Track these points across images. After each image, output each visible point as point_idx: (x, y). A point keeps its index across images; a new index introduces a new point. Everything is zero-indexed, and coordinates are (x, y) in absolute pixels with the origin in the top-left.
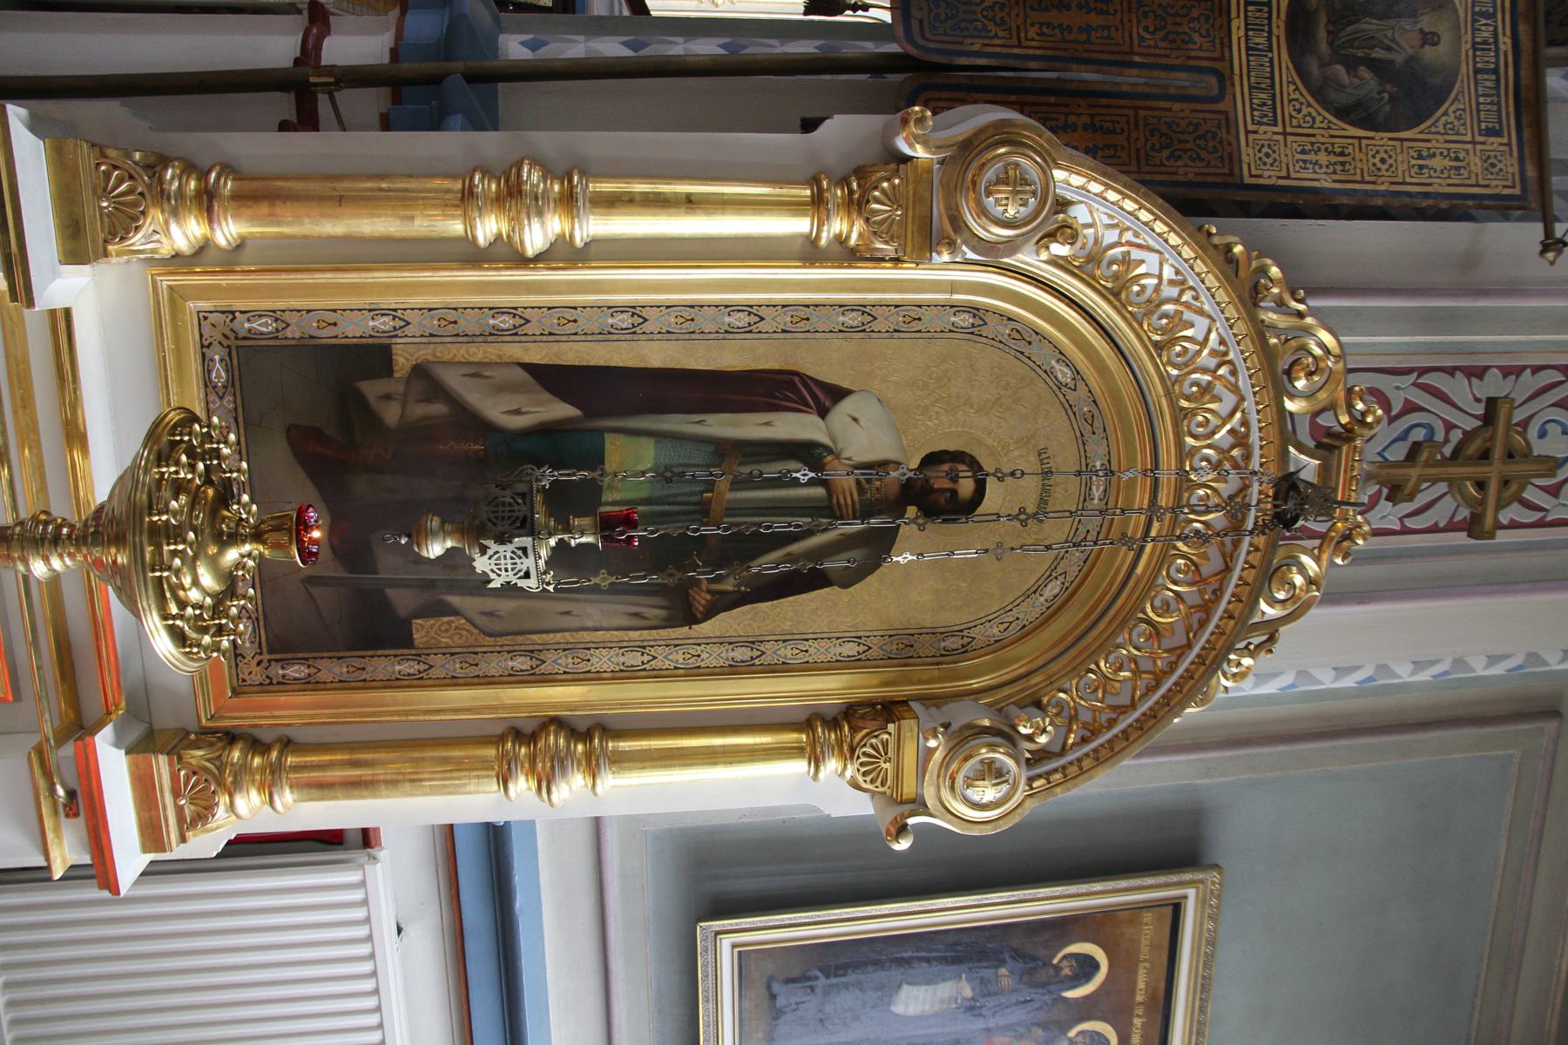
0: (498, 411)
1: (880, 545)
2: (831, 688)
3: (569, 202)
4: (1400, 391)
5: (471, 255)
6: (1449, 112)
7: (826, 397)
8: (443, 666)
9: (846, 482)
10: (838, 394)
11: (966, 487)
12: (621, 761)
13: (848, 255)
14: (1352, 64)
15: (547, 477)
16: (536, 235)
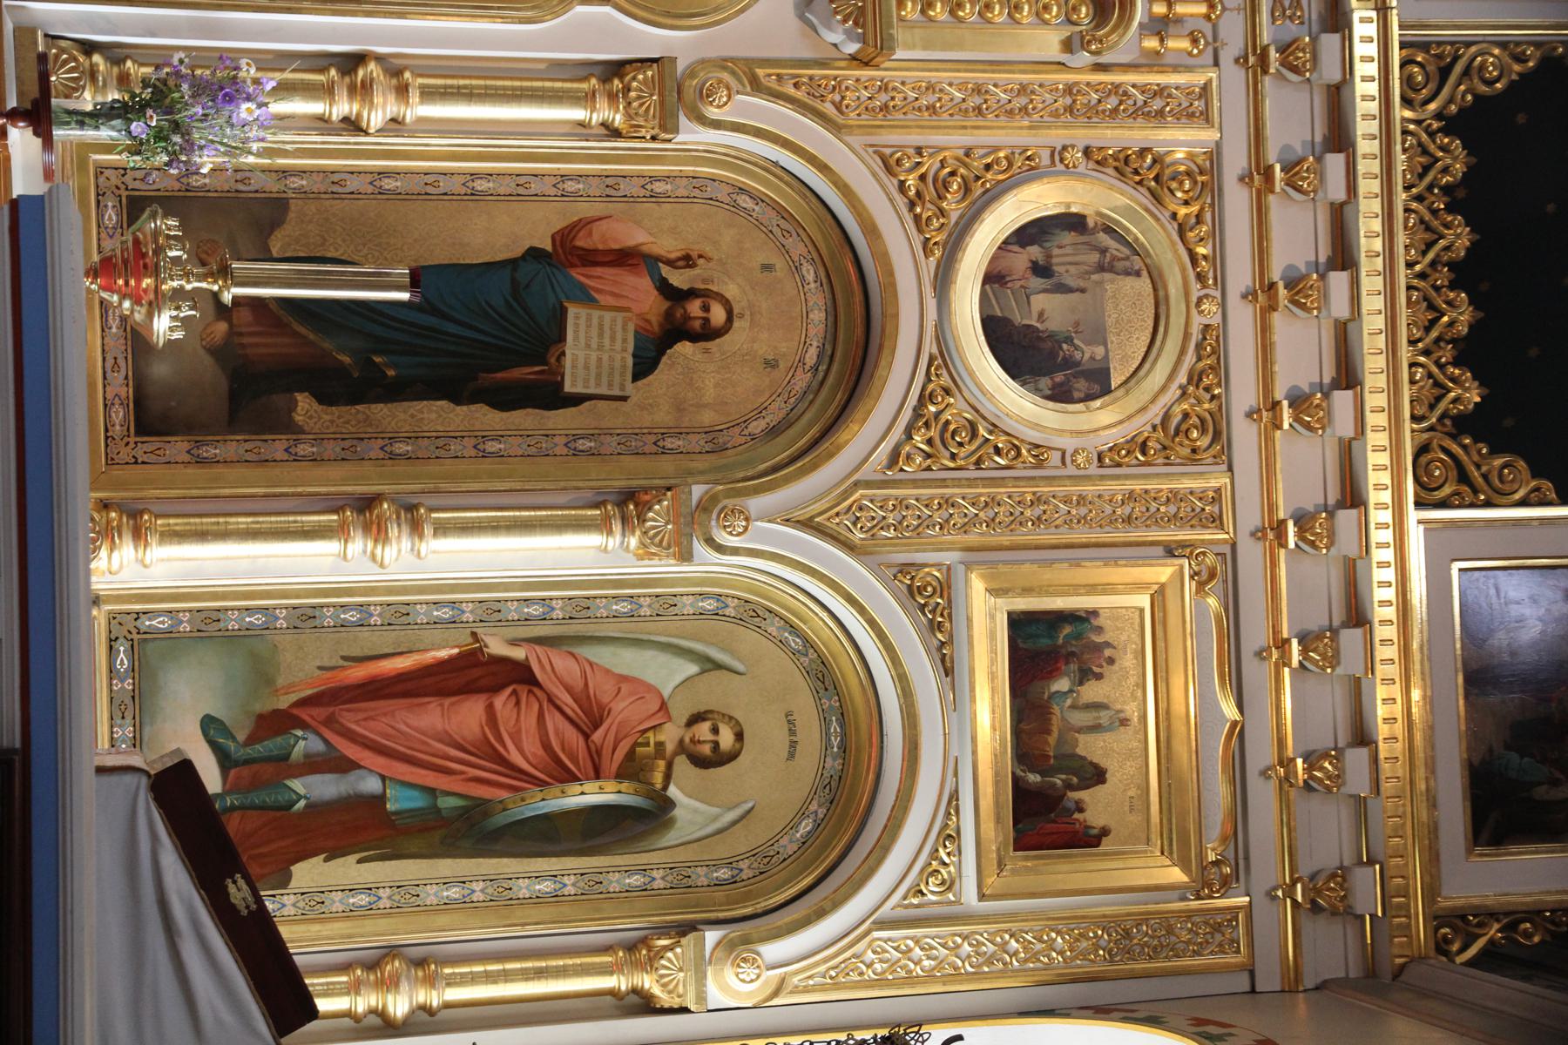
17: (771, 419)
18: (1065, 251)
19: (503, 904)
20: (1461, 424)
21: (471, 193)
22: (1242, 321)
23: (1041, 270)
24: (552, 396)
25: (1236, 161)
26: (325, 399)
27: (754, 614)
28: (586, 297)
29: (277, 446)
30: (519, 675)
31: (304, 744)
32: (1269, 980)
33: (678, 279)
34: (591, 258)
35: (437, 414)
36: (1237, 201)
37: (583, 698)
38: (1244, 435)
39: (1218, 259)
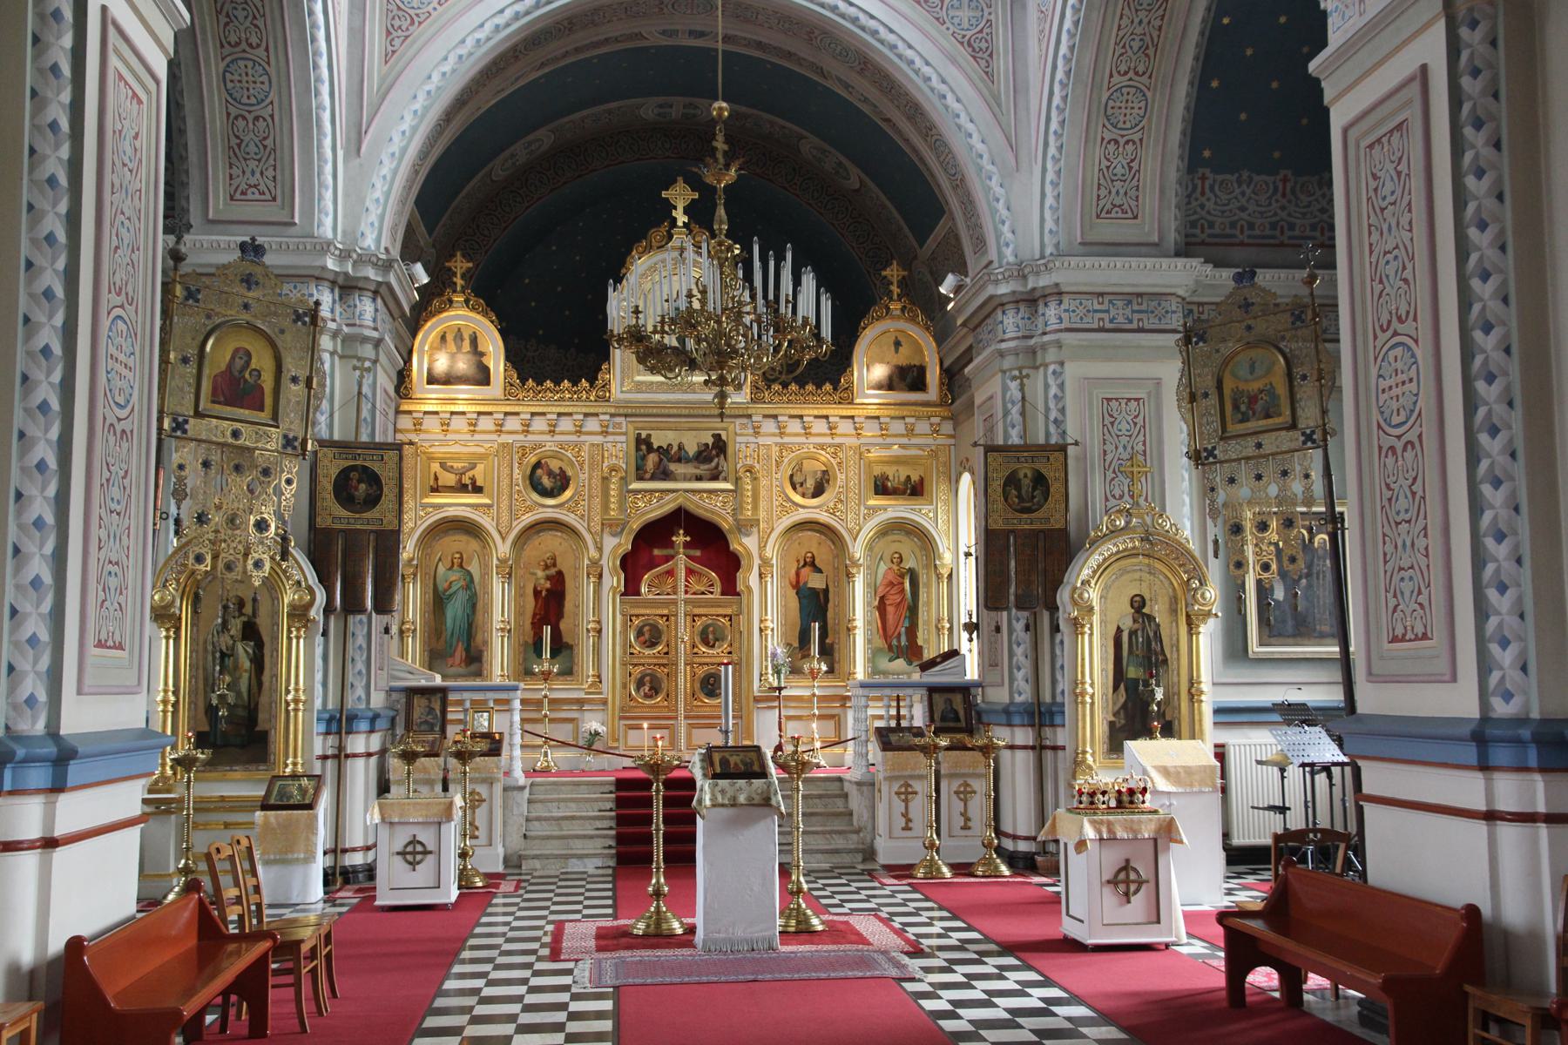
0: (1122, 700)
1: (1151, 618)
2: (1183, 629)
3: (1083, 683)
4: (1110, 475)
5: (1092, 704)
6: (1043, 471)
7: (1119, 630)
8: (1176, 715)
10: (1118, 628)
11: (1137, 599)
12: (1198, 676)
13: (1091, 629)
14: (1033, 497)
15: (1141, 688)
16: (1090, 690)
17: (830, 543)
18: (797, 479)
19: (928, 603)
20: (835, 389)
21: (785, 606)
22: (812, 440)
23: (802, 485)
24: (826, 591)
25: (778, 440)
26: (827, 637)
27: (870, 547)
28: (806, 583)
29: (836, 646)
30: (882, 599)
31: (895, 642)
32: (952, 441)
33: (802, 563)
34: (798, 582)
35: (830, 614)
36: (786, 440)
37: (887, 586)
38: (837, 440)
39: (799, 444)
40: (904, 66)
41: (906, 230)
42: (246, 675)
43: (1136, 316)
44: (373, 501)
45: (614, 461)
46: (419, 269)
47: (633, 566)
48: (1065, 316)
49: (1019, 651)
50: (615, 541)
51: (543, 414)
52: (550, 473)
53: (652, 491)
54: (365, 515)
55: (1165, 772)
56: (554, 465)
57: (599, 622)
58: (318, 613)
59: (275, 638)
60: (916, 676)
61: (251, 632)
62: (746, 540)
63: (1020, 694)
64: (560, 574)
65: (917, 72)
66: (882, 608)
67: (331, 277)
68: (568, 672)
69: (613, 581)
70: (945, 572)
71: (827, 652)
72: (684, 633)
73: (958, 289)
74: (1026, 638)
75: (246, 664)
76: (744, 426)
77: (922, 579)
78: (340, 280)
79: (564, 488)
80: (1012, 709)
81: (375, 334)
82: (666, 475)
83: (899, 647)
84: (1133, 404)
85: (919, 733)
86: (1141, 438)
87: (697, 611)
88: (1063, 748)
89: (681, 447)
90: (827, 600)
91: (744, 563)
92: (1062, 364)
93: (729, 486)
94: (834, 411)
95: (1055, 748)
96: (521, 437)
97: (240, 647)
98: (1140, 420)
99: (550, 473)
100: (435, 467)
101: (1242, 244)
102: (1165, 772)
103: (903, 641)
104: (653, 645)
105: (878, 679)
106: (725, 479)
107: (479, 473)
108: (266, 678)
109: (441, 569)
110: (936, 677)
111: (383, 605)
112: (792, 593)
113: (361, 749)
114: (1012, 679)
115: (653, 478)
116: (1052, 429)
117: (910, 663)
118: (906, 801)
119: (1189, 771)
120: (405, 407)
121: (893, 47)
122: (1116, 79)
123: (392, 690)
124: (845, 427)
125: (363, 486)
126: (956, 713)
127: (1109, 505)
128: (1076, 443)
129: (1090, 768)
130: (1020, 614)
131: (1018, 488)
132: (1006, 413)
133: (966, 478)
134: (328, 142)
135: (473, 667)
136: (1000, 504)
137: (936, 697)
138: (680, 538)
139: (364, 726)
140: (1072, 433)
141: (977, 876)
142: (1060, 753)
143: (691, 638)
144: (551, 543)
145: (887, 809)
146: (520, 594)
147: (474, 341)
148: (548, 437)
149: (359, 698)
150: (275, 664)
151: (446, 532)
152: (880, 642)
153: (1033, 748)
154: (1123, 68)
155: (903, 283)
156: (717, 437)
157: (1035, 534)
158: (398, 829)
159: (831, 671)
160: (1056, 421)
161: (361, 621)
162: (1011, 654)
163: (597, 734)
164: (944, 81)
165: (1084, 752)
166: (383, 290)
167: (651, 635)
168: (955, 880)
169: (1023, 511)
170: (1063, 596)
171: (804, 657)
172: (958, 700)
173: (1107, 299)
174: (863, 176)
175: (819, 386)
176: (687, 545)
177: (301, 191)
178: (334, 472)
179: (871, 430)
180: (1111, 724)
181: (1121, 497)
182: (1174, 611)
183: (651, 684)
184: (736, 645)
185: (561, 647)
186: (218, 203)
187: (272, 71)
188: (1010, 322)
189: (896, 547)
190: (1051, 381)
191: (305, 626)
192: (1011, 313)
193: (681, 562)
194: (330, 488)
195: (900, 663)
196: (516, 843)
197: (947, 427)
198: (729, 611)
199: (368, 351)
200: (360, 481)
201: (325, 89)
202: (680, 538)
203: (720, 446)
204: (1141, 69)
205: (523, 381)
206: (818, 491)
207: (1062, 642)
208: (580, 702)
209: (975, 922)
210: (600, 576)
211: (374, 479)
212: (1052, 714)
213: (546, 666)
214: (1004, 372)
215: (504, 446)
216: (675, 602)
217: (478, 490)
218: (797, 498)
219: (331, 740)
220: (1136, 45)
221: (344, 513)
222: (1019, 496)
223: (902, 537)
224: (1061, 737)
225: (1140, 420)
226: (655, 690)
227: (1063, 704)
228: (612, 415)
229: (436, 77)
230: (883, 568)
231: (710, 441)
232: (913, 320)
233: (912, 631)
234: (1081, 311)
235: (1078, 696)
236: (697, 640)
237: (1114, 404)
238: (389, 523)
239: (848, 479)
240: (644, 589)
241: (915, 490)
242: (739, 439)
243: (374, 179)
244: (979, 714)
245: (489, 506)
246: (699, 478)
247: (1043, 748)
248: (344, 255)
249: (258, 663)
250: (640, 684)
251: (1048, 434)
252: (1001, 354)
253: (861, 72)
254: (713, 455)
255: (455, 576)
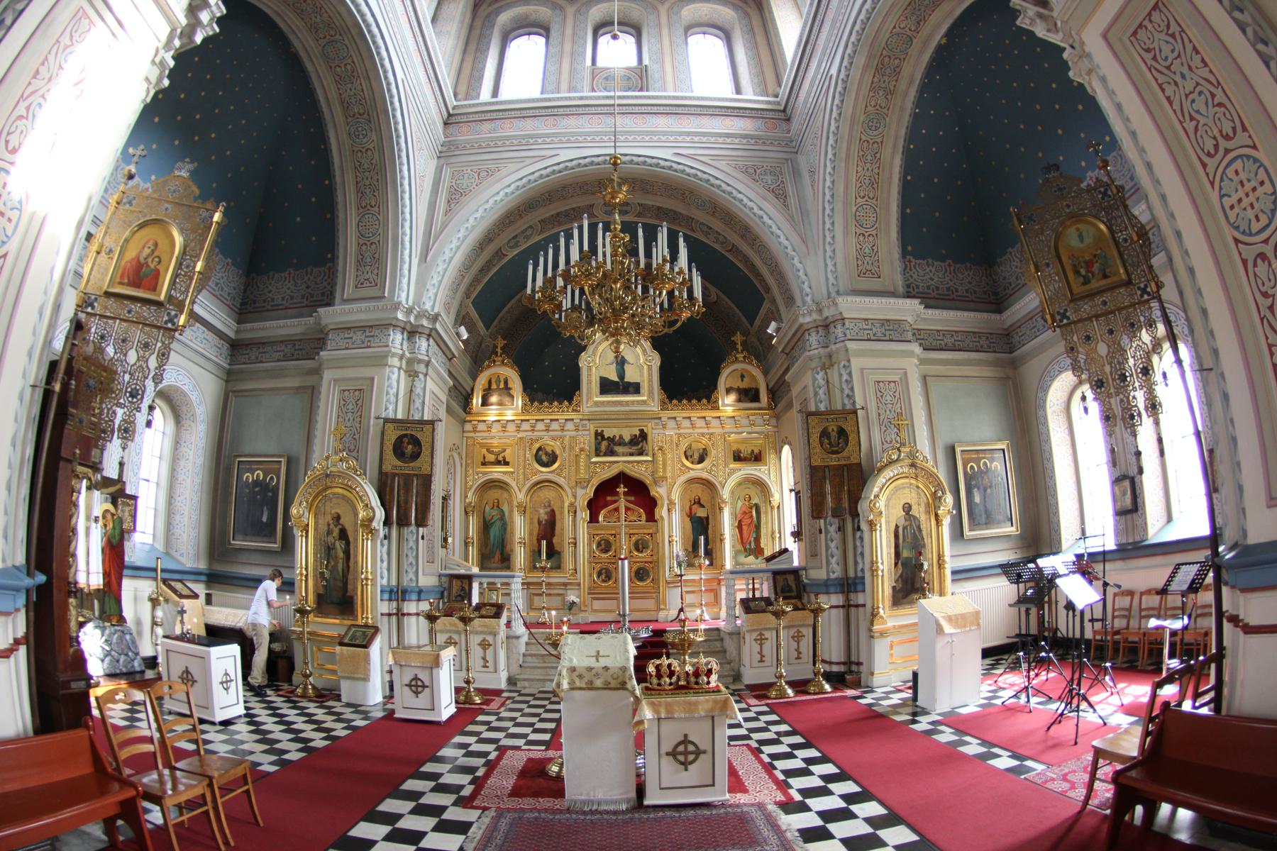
0: (900, 572)
1: (915, 517)
3: (877, 563)
4: (883, 428)
6: (844, 427)
7: (897, 527)
9: (907, 523)
16: (881, 567)
18: (689, 453)
19: (767, 523)
22: (697, 431)
24: (707, 518)
25: (677, 431)
27: (732, 492)
30: (740, 521)
35: (710, 532)
36: (682, 431)
40: (737, 203)
41: (743, 318)
42: (341, 561)
43: (888, 333)
44: (415, 456)
45: (582, 446)
46: (463, 330)
47: (594, 506)
48: (848, 332)
49: (833, 545)
50: (584, 491)
51: (543, 420)
52: (547, 454)
53: (604, 463)
54: (411, 465)
55: (950, 619)
56: (549, 449)
57: (575, 539)
58: (379, 525)
59: (356, 540)
60: (763, 566)
61: (343, 534)
62: (659, 490)
63: (834, 573)
64: (553, 511)
65: (745, 206)
66: (740, 527)
67: (402, 325)
68: (558, 567)
69: (584, 515)
70: (775, 504)
71: (709, 553)
72: (625, 545)
73: (778, 330)
74: (837, 536)
75: (341, 555)
76: (657, 424)
77: (763, 510)
78: (408, 327)
79: (554, 461)
80: (829, 583)
81: (426, 358)
82: (613, 453)
83: (750, 549)
84: (892, 384)
85: (768, 601)
86: (899, 405)
87: (632, 531)
88: (864, 605)
89: (621, 437)
90: (708, 524)
91: (659, 502)
92: (849, 361)
93: (649, 458)
94: (710, 414)
95: (857, 606)
96: (530, 433)
97: (338, 543)
98: (897, 394)
99: (547, 454)
100: (484, 451)
101: (934, 298)
102: (950, 619)
103: (753, 546)
104: (606, 551)
105: (739, 568)
106: (647, 455)
107: (508, 455)
108: (351, 564)
109: (488, 508)
110: (776, 565)
111: (422, 522)
112: (688, 520)
113: (414, 611)
114: (828, 563)
115: (605, 455)
116: (846, 401)
117: (757, 558)
118: (761, 644)
119: (963, 616)
120: (468, 419)
121: (730, 193)
122: (859, 200)
123: (440, 576)
124: (715, 423)
125: (410, 447)
126: (789, 586)
127: (885, 447)
128: (863, 408)
129: (882, 617)
130: (832, 520)
131: (829, 439)
132: (816, 394)
133: (786, 449)
134: (407, 252)
135: (505, 564)
136: (818, 449)
137: (778, 577)
138: (622, 489)
139: (414, 597)
140: (859, 403)
141: (810, 694)
142: (861, 609)
143: (629, 547)
144: (548, 494)
145: (750, 648)
146: (531, 523)
147: (506, 382)
148: (545, 433)
149: (411, 580)
150: (356, 556)
151: (490, 488)
152: (739, 547)
153: (843, 607)
154: (862, 194)
155: (744, 344)
156: (642, 431)
157: (841, 467)
158: (404, 668)
159: (711, 564)
160: (848, 396)
161: (412, 532)
162: (827, 547)
163: (574, 603)
164: (761, 209)
165: (878, 608)
166: (433, 333)
167: (605, 546)
168: (798, 699)
169: (833, 453)
170: (863, 507)
171: (695, 557)
172: (791, 578)
173: (870, 322)
174: (718, 291)
175: (699, 401)
176: (625, 494)
177: (390, 279)
178: (394, 438)
179: (729, 426)
180: (894, 588)
181: (891, 442)
182: (928, 512)
183: (607, 574)
184: (655, 551)
185: (553, 553)
186: (349, 291)
187: (380, 218)
188: (813, 339)
189: (747, 491)
190: (843, 372)
191: (371, 532)
192: (814, 334)
193: (622, 503)
194: (391, 448)
195: (751, 558)
196: (515, 669)
197: (773, 421)
198: (651, 531)
199: (422, 368)
200: (409, 443)
201: (407, 225)
202: (622, 489)
203: (643, 436)
204: (871, 196)
205: (532, 401)
206: (701, 460)
207: (861, 538)
208: (565, 584)
209: (832, 750)
210: (575, 512)
211: (416, 442)
212: (855, 584)
213: (543, 563)
214: (813, 370)
215: (521, 439)
216: (620, 527)
217: (507, 463)
218: (688, 464)
219: (394, 604)
220: (867, 182)
221: (399, 463)
222: (830, 443)
223: (750, 486)
224: (860, 598)
225: (897, 394)
226: (608, 577)
227: (863, 578)
228: (581, 420)
229: (471, 220)
230: (740, 504)
231: (638, 433)
232: (751, 363)
233: (757, 540)
234: (856, 329)
235: (874, 571)
236: (632, 548)
237: (881, 384)
238: (425, 469)
239: (718, 454)
240: (601, 519)
241: (757, 458)
242: (655, 431)
243: (433, 273)
244: (804, 586)
245: (512, 473)
246: (632, 455)
247: (850, 606)
248: (409, 311)
249: (347, 553)
250: (599, 574)
251: (844, 405)
252: (811, 359)
253: (713, 215)
254: (639, 442)
255: (494, 512)
